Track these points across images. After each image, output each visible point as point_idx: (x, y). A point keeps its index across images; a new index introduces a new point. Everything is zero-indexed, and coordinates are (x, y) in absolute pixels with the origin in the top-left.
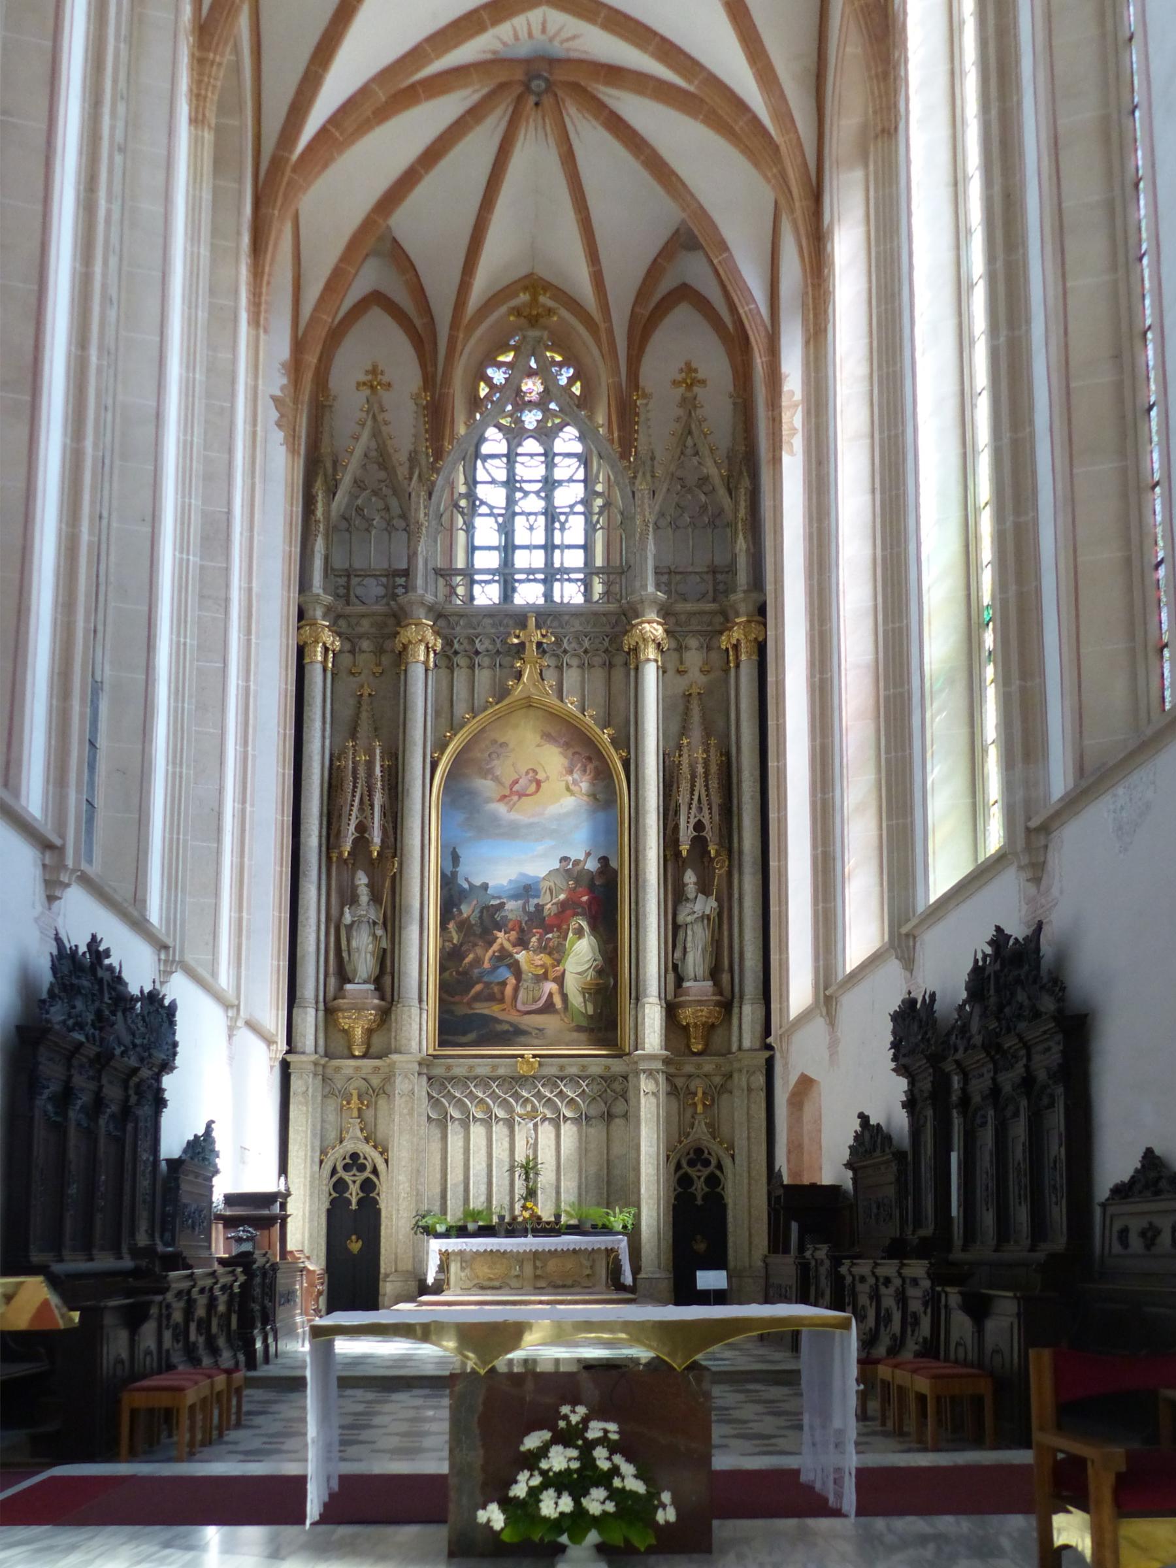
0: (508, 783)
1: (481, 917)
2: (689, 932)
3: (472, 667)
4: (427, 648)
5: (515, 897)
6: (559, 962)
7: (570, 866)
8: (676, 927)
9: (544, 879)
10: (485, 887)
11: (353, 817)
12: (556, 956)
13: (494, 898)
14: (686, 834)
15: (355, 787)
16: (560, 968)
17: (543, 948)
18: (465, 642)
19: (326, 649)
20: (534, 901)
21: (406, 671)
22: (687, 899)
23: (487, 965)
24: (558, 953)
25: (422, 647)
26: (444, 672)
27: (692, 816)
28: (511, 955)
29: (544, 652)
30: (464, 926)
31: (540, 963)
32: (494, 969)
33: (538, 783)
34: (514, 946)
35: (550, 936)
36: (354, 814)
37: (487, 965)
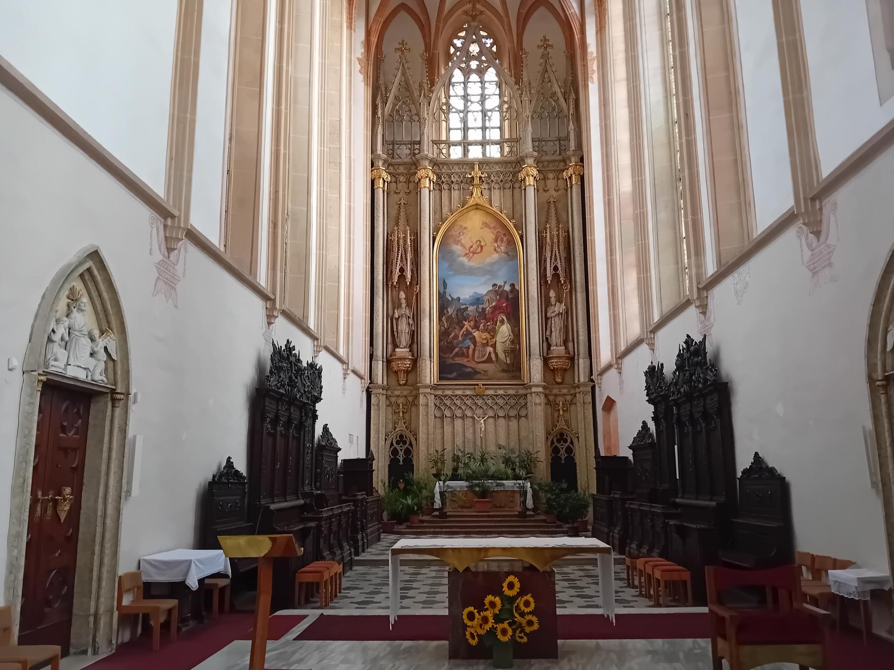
0: (468, 247)
1: (457, 315)
2: (553, 322)
3: (450, 190)
4: (430, 180)
5: (472, 304)
6: (493, 337)
7: (497, 289)
8: (547, 319)
9: (485, 295)
10: (459, 299)
11: (398, 265)
12: (492, 334)
13: (463, 305)
14: (549, 273)
15: (398, 250)
16: (494, 340)
17: (486, 330)
18: (447, 177)
19: (384, 181)
20: (481, 306)
21: (420, 191)
22: (552, 305)
23: (460, 338)
24: (493, 332)
26: (438, 192)
27: (552, 263)
28: (471, 334)
29: (483, 182)
30: (449, 318)
31: (484, 337)
32: (464, 340)
33: (482, 247)
34: (472, 329)
35: (489, 323)
36: (398, 263)
37: (460, 338)
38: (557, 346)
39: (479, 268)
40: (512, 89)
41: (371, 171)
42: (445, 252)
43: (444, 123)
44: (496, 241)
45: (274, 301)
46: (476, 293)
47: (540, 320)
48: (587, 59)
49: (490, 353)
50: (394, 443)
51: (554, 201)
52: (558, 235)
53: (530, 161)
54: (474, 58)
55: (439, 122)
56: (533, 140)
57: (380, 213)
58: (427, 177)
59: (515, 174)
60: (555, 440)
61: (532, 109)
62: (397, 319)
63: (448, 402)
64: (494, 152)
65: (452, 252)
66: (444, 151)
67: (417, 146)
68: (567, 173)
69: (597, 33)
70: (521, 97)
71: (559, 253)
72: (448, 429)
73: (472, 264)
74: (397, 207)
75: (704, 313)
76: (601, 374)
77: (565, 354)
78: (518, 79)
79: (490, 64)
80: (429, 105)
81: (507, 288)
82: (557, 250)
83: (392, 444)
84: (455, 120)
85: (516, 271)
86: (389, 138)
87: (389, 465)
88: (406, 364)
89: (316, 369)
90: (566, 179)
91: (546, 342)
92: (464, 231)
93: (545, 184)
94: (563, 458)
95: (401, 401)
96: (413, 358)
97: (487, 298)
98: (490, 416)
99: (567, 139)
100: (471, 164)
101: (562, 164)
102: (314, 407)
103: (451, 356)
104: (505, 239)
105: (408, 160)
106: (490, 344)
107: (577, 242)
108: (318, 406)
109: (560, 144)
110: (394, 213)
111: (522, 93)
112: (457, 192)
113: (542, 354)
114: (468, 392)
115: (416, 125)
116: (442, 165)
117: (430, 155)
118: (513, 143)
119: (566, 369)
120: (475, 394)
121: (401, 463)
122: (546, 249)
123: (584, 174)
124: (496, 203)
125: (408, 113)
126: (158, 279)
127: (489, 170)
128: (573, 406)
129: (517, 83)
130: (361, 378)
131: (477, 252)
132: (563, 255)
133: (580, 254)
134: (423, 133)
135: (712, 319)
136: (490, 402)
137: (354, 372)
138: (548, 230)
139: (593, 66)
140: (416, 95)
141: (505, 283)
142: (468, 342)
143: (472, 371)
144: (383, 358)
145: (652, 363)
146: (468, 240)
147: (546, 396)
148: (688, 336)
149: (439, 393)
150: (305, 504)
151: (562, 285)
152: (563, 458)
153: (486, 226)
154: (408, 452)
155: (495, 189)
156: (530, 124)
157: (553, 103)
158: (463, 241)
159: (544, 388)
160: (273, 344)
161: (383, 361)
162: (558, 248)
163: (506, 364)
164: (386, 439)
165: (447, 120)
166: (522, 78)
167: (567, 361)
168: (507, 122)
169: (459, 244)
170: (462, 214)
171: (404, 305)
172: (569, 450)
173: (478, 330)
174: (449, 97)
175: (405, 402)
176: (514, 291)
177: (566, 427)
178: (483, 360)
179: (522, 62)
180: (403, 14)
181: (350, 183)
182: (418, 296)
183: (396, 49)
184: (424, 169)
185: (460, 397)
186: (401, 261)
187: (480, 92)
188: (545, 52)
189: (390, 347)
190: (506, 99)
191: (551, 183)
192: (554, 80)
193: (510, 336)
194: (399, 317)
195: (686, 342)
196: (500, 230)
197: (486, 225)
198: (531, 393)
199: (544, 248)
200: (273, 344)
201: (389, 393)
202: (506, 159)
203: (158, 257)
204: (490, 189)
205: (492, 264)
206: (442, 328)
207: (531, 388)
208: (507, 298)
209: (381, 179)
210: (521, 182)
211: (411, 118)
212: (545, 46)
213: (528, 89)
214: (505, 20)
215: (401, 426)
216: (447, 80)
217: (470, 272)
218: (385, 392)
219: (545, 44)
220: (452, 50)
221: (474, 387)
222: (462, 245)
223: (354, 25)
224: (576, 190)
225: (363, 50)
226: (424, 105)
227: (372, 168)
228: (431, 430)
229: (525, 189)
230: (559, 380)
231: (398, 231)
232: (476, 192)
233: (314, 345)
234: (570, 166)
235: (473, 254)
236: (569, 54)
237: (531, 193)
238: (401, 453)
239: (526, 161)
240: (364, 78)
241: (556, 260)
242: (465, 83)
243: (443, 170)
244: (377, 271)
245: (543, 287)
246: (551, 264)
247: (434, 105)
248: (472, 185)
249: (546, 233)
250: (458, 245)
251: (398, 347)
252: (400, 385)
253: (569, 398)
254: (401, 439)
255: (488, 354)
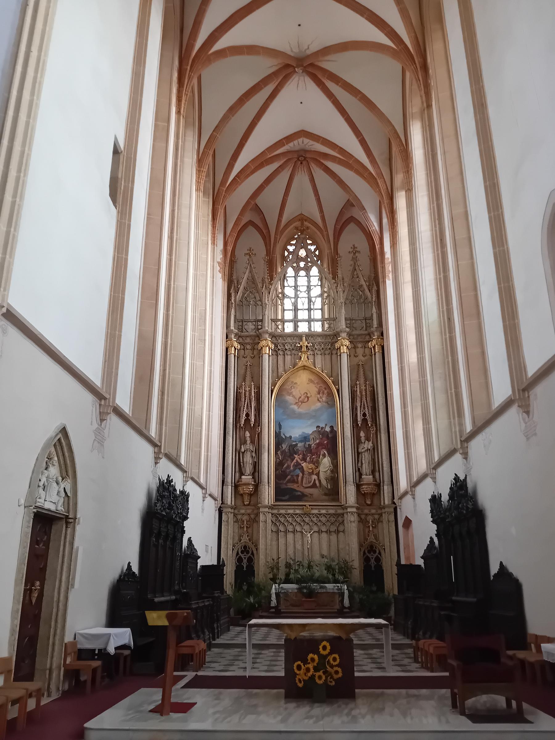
2: (363, 456)
3: (284, 355)
4: (269, 348)
5: (301, 441)
6: (317, 467)
7: (320, 430)
8: (358, 453)
9: (311, 434)
10: (291, 437)
12: (316, 465)
13: (294, 442)
14: (360, 418)
15: (245, 400)
16: (318, 470)
17: (312, 462)
19: (235, 349)
20: (307, 443)
21: (262, 356)
23: (292, 468)
24: (317, 464)
25: (268, 348)
26: (275, 356)
27: (362, 411)
29: (309, 349)
30: (283, 452)
31: (311, 467)
32: (294, 470)
33: (308, 398)
34: (301, 461)
35: (314, 457)
37: (292, 468)
38: (366, 475)
39: (306, 413)
40: (330, 283)
41: (226, 341)
42: (280, 402)
43: (280, 307)
44: (319, 394)
45: (160, 447)
46: (303, 433)
47: (353, 455)
48: (385, 263)
49: (315, 480)
50: (240, 553)
51: (362, 364)
52: (366, 390)
53: (344, 335)
54: (302, 259)
55: (276, 306)
56: (346, 319)
57: (232, 373)
58: (267, 346)
59: (333, 344)
60: (366, 551)
61: (345, 297)
62: (243, 453)
63: (282, 520)
64: (317, 327)
65: (286, 402)
66: (280, 327)
67: (260, 323)
68: (371, 343)
69: (391, 247)
70: (336, 288)
71: (366, 403)
72: (282, 541)
73: (300, 410)
74: (244, 367)
75: (466, 458)
76: (401, 498)
77: (373, 481)
78: (335, 276)
79: (314, 263)
80: (269, 294)
81: (328, 429)
82: (365, 401)
83: (238, 554)
84: (288, 304)
85: (334, 416)
86: (239, 317)
87: (235, 570)
88: (249, 488)
89: (185, 495)
90: (371, 348)
91: (358, 472)
92: (295, 386)
93: (356, 351)
94: (373, 566)
95: (245, 518)
96: (255, 484)
97: (312, 437)
98: (315, 531)
99: (371, 318)
100: (300, 337)
101: (368, 337)
102: (183, 524)
103: (284, 482)
104: (325, 392)
105: (253, 333)
106: (315, 473)
107: (380, 395)
108: (186, 523)
109: (366, 322)
110: (242, 372)
111: (337, 286)
112: (289, 357)
113: (355, 481)
114: (298, 512)
115: (259, 308)
116: (279, 337)
117: (270, 330)
118: (331, 321)
119: (374, 494)
120: (303, 513)
121: (245, 569)
122: (356, 400)
123: (384, 345)
124: (319, 365)
125: (254, 299)
126: (95, 440)
127: (314, 341)
128: (380, 524)
129: (334, 278)
130: (215, 499)
131: (305, 401)
132: (370, 405)
133: (383, 404)
134: (265, 314)
135: (471, 463)
136: (315, 519)
137: (210, 495)
138: (358, 386)
139: (389, 268)
140: (259, 287)
141: (326, 425)
142: (298, 472)
143: (301, 494)
144: (232, 483)
145: (434, 493)
146: (297, 392)
147: (359, 515)
148: (456, 474)
149: (275, 511)
150: (176, 599)
151: (370, 427)
152: (373, 566)
153: (311, 382)
154: (250, 560)
155: (318, 354)
156: (343, 308)
157: (361, 293)
158: (294, 394)
159: (357, 508)
160: (159, 479)
161: (232, 486)
162: (366, 399)
163: (327, 489)
164: (233, 549)
165: (282, 304)
166: (337, 275)
167: (375, 487)
168: (326, 306)
169: (291, 395)
170: (293, 373)
171: (248, 442)
172: (378, 560)
173: (305, 462)
174: (284, 287)
175: (248, 519)
176: (333, 431)
177: (374, 541)
178: (309, 485)
179: (338, 263)
180: (251, 228)
181: (211, 353)
182: (260, 435)
183: (245, 254)
184: (265, 340)
185: (292, 515)
186: (247, 408)
187: (306, 284)
188: (354, 256)
189: (237, 475)
190: (326, 290)
191: (360, 351)
192: (361, 276)
193: (330, 466)
194: (245, 451)
195: (454, 479)
196: (322, 385)
197: (311, 381)
198: (347, 513)
199: (355, 399)
200: (159, 479)
201: (236, 511)
202: (326, 333)
203: (95, 426)
204: (314, 355)
205: (316, 411)
206: (278, 460)
207: (347, 509)
208: (327, 437)
209: (233, 347)
210: (337, 350)
211: (256, 303)
212: (354, 252)
213: (342, 283)
214: (325, 233)
215: (245, 539)
216: (283, 276)
217: (300, 416)
218: (233, 511)
219: (355, 251)
220: (286, 253)
221: (302, 507)
222: (294, 396)
223: (217, 242)
224: (378, 357)
225: (222, 256)
226: (266, 294)
227: (226, 339)
228: (269, 542)
229: (340, 355)
230: (369, 502)
231: (245, 386)
232: (304, 357)
233: (184, 477)
234: (374, 339)
235: (302, 403)
236: (372, 258)
237: (345, 358)
238: (245, 561)
239: (341, 335)
240: (222, 276)
241: (364, 408)
242: (296, 277)
243: (279, 341)
244: (228, 416)
245: (355, 429)
246: (360, 411)
247: (273, 294)
248: (301, 352)
249: (357, 388)
250: (290, 396)
251: (243, 475)
252: (245, 505)
253: (376, 517)
254: (245, 550)
255: (313, 481)
